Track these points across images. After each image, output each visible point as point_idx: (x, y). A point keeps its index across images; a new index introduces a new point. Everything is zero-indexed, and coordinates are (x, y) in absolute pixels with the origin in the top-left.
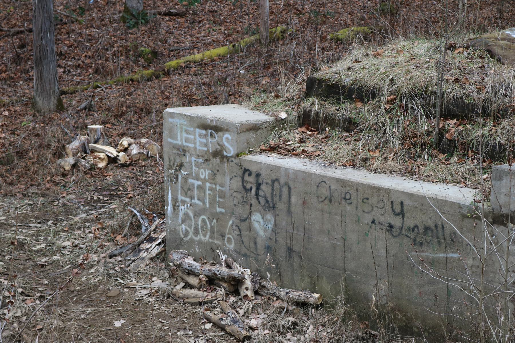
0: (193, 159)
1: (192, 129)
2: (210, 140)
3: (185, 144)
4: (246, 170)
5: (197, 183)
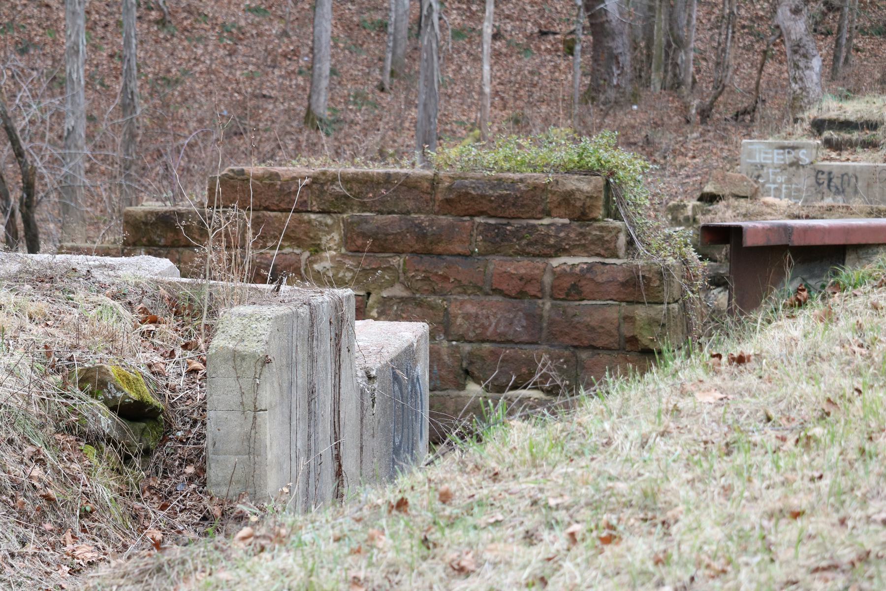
0: (771, 171)
1: (770, 151)
2: (787, 155)
3: (763, 161)
4: (819, 171)
5: (773, 186)
